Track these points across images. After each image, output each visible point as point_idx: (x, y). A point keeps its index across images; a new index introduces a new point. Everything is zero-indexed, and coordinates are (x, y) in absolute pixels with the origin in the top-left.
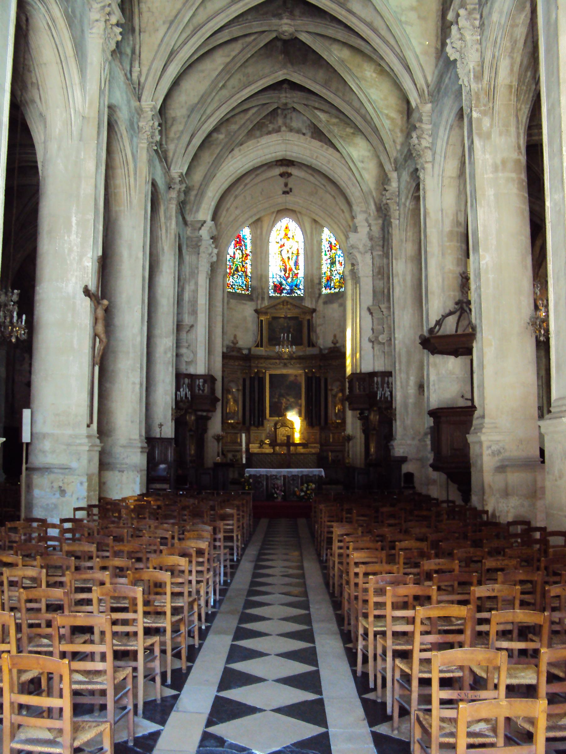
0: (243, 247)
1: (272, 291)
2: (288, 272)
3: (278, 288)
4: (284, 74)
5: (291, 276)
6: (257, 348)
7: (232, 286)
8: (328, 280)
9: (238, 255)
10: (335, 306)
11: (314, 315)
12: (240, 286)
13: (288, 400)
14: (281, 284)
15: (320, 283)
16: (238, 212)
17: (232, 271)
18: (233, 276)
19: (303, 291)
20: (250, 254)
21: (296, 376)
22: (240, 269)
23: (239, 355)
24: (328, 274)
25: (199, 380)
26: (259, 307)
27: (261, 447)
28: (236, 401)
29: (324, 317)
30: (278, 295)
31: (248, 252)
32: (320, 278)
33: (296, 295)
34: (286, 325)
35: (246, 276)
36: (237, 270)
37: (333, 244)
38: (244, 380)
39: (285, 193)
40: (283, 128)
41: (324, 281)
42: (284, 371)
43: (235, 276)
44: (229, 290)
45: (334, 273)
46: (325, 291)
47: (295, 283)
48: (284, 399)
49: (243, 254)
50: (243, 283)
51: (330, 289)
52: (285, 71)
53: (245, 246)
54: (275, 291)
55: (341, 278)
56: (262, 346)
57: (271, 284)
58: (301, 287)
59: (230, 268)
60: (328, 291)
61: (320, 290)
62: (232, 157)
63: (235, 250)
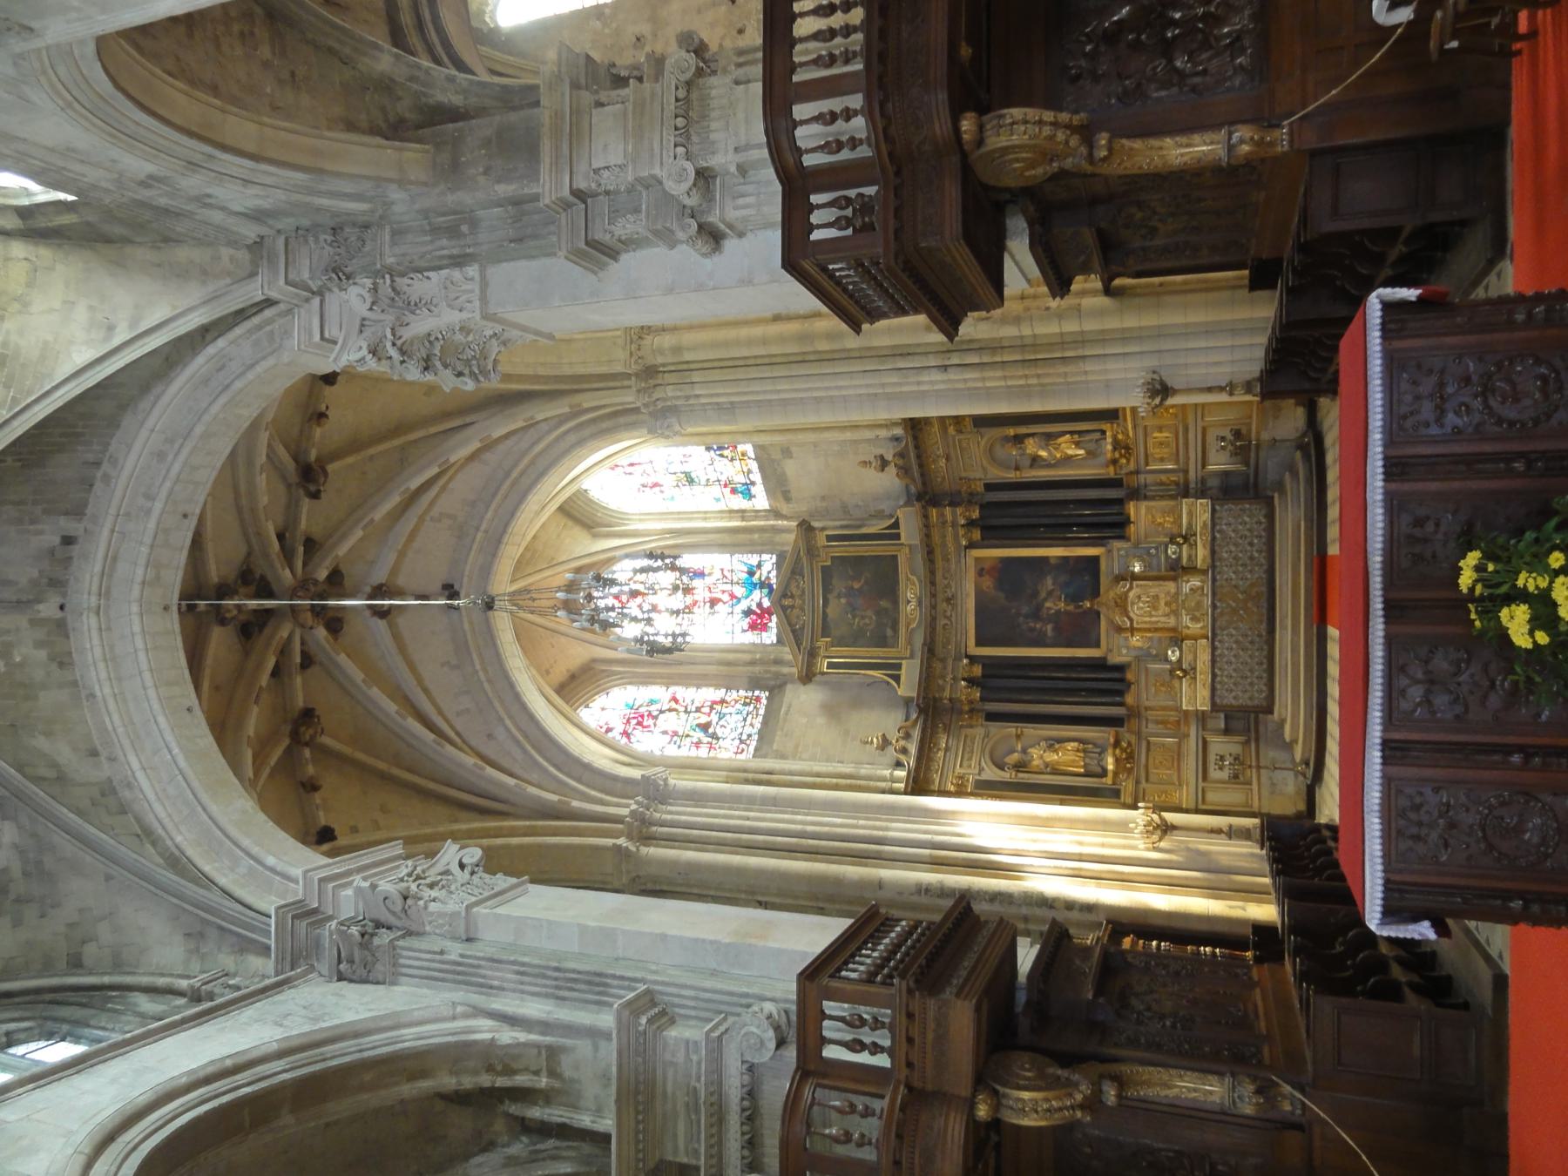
0: (652, 708)
2: (719, 595)
3: (757, 620)
5: (728, 587)
6: (903, 679)
7: (742, 742)
8: (733, 491)
9: (669, 722)
10: (790, 467)
11: (816, 524)
12: (745, 720)
13: (1050, 593)
14: (748, 612)
15: (742, 514)
16: (500, 733)
19: (765, 557)
20: (673, 689)
21: (980, 573)
22: (704, 719)
24: (716, 490)
25: (824, 1041)
26: (794, 670)
27: (1190, 672)
28: (1054, 743)
29: (823, 498)
31: (668, 695)
32: (732, 513)
33: (774, 573)
34: (843, 601)
35: (723, 702)
36: (705, 727)
37: (645, 480)
38: (992, 717)
40: (48, 609)
41: (738, 502)
42: (971, 604)
43: (719, 732)
44: (752, 749)
45: (713, 477)
46: (761, 501)
47: (746, 576)
48: (1048, 604)
49: (670, 710)
51: (753, 483)
53: (652, 702)
54: (764, 628)
55: (722, 456)
56: (898, 667)
57: (751, 638)
58: (753, 560)
59: (698, 744)
60: (759, 490)
61: (757, 514)
62: (129, 786)
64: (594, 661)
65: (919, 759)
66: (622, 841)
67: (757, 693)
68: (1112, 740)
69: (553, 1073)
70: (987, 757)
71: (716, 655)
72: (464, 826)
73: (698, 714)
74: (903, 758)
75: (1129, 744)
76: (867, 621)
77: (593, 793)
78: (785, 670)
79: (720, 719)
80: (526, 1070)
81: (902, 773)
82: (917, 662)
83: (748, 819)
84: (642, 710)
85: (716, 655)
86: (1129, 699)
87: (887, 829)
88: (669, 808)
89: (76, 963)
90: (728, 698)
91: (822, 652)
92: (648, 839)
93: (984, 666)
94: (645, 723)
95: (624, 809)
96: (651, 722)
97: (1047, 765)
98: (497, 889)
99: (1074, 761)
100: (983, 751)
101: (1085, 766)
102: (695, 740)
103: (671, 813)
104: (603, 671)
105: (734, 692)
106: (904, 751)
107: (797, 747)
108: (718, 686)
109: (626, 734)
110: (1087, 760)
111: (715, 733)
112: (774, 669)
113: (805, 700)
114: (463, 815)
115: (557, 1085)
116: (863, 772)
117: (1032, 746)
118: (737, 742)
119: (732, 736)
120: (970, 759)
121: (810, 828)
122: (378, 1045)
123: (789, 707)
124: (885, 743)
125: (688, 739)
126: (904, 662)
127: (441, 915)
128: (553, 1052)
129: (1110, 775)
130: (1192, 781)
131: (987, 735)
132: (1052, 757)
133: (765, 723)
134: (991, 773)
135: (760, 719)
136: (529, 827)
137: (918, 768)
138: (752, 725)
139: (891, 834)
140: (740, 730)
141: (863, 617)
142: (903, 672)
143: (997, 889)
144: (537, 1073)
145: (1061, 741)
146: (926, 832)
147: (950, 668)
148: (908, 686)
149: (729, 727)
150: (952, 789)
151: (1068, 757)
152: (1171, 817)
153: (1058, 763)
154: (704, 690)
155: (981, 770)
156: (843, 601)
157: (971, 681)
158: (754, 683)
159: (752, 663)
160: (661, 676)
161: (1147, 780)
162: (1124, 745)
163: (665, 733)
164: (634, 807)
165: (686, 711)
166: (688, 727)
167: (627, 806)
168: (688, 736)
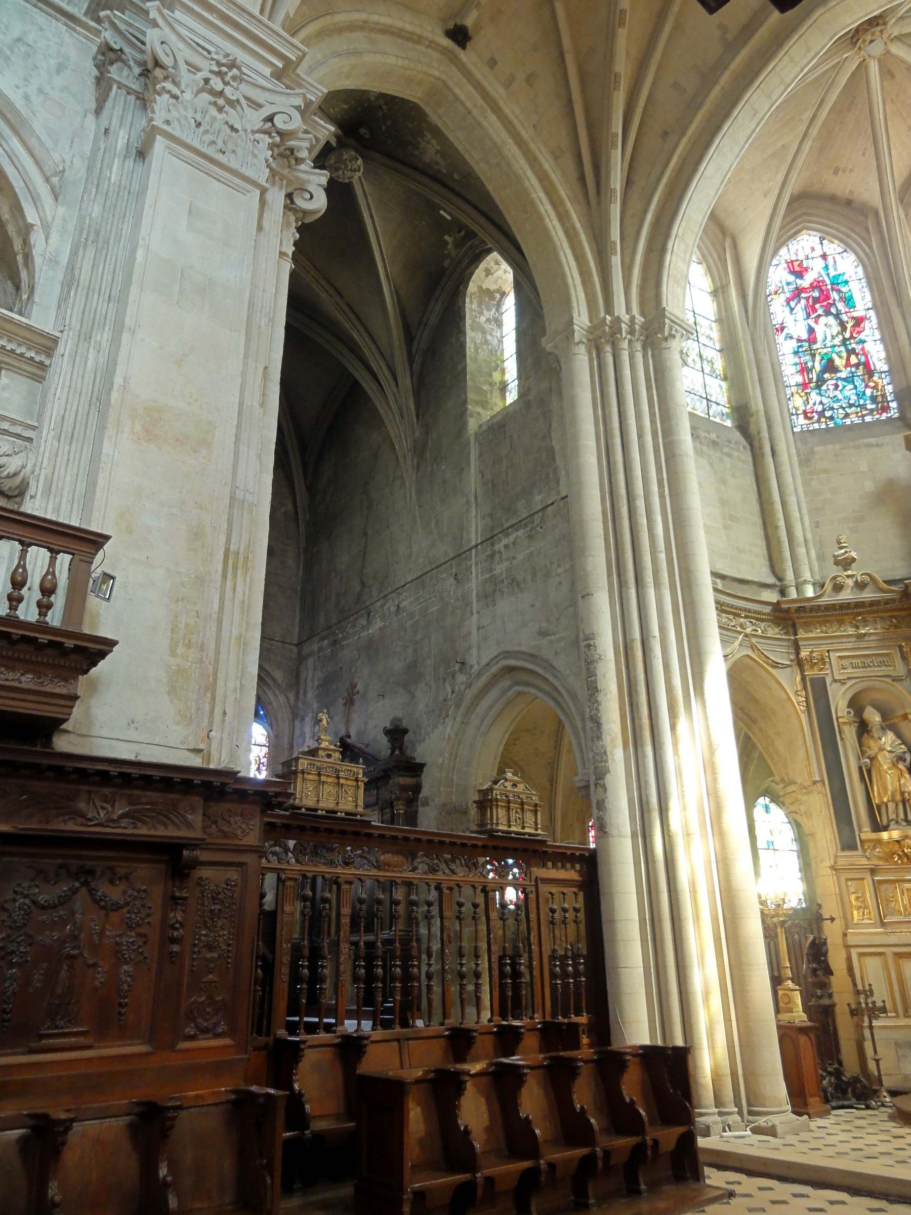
0: (841, 306)
7: (821, 414)
12: (851, 406)
17: (814, 376)
18: (818, 387)
20: (872, 313)
22: (839, 362)
23: (868, 595)
35: (870, 372)
53: (848, 301)
63: (811, 322)
64: (876, 213)
67: (894, 405)
73: (844, 355)
74: (828, 586)
79: (845, 380)
81: (810, 592)
83: (640, 436)
84: (834, 295)
87: (657, 585)
88: (639, 356)
90: (875, 378)
92: (595, 346)
94: (817, 306)
96: (820, 312)
99: (886, 789)
102: (810, 364)
103: (632, 357)
104: (867, 229)
105: (888, 380)
106: (838, 588)
107: (825, 471)
108: (888, 359)
109: (798, 292)
110: (891, 806)
111: (825, 381)
114: (569, 162)
116: (801, 551)
117: (899, 735)
118: (820, 408)
119: (825, 400)
121: (641, 504)
123: (877, 445)
124: (846, 563)
125: (808, 358)
129: (874, 836)
130: (893, 939)
131: (895, 679)
132: (884, 762)
133: (853, 426)
135: (857, 421)
136: (574, 228)
137: (818, 608)
138: (847, 415)
139: (651, 593)
140: (836, 406)
143: (604, 720)
146: (662, 629)
149: (837, 393)
150: (804, 654)
154: (881, 347)
155: (842, 682)
160: (881, 293)
163: (811, 331)
165: (844, 341)
166: (825, 351)
168: (813, 356)
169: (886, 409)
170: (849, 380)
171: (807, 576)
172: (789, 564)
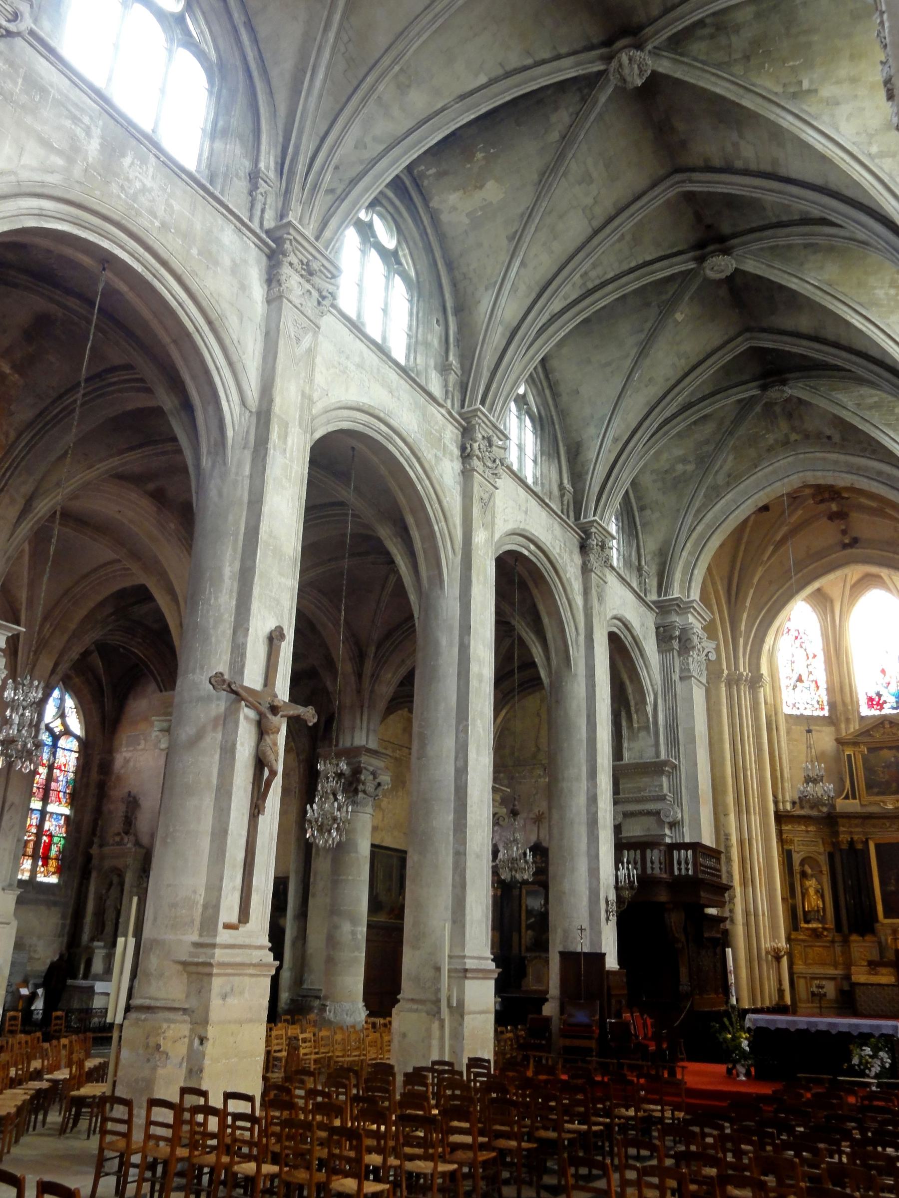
1: (866, 706)
3: (875, 702)
4: (747, 340)
6: (847, 801)
9: (800, 655)
14: (879, 695)
22: (804, 678)
23: (814, 813)
26: (844, 734)
28: (821, 894)
30: (877, 713)
36: (800, 679)
38: (831, 856)
39: (845, 546)
50: (812, 699)
52: (748, 335)
56: (854, 798)
64: (832, 602)
65: (799, 817)
66: (726, 672)
67: (827, 708)
68: (827, 926)
69: (639, 729)
70: (807, 855)
71: (847, 681)
72: (720, 587)
75: (826, 936)
76: (882, 775)
77: (749, 648)
78: (843, 726)
80: (638, 718)
81: (788, 807)
82: (859, 809)
83: (748, 737)
85: (847, 681)
86: (854, 937)
87: (755, 814)
89: (642, 509)
91: (857, 749)
92: (729, 685)
93: (862, 850)
95: (743, 669)
97: (807, 890)
98: (700, 679)
100: (809, 852)
101: (809, 911)
103: (745, 694)
107: (796, 741)
112: (843, 718)
113: (825, 740)
115: (636, 730)
120: (803, 845)
122: (639, 663)
126: (857, 801)
127: (688, 664)
128: (647, 728)
130: (810, 971)
131: (820, 854)
132: (812, 891)
134: (797, 858)
137: (793, 816)
141: (883, 772)
142: (851, 801)
144: (638, 722)
145: (822, 897)
147: (857, 829)
148: (843, 805)
151: (813, 901)
152: (785, 961)
153: (809, 896)
155: (798, 853)
156: (893, 759)
157: (852, 843)
158: (832, 706)
159: (844, 704)
161: (805, 946)
162: (825, 933)
164: (745, 674)
167: (745, 670)
169: (822, 709)
170: (809, 688)
171: (788, 798)
172: (780, 790)
